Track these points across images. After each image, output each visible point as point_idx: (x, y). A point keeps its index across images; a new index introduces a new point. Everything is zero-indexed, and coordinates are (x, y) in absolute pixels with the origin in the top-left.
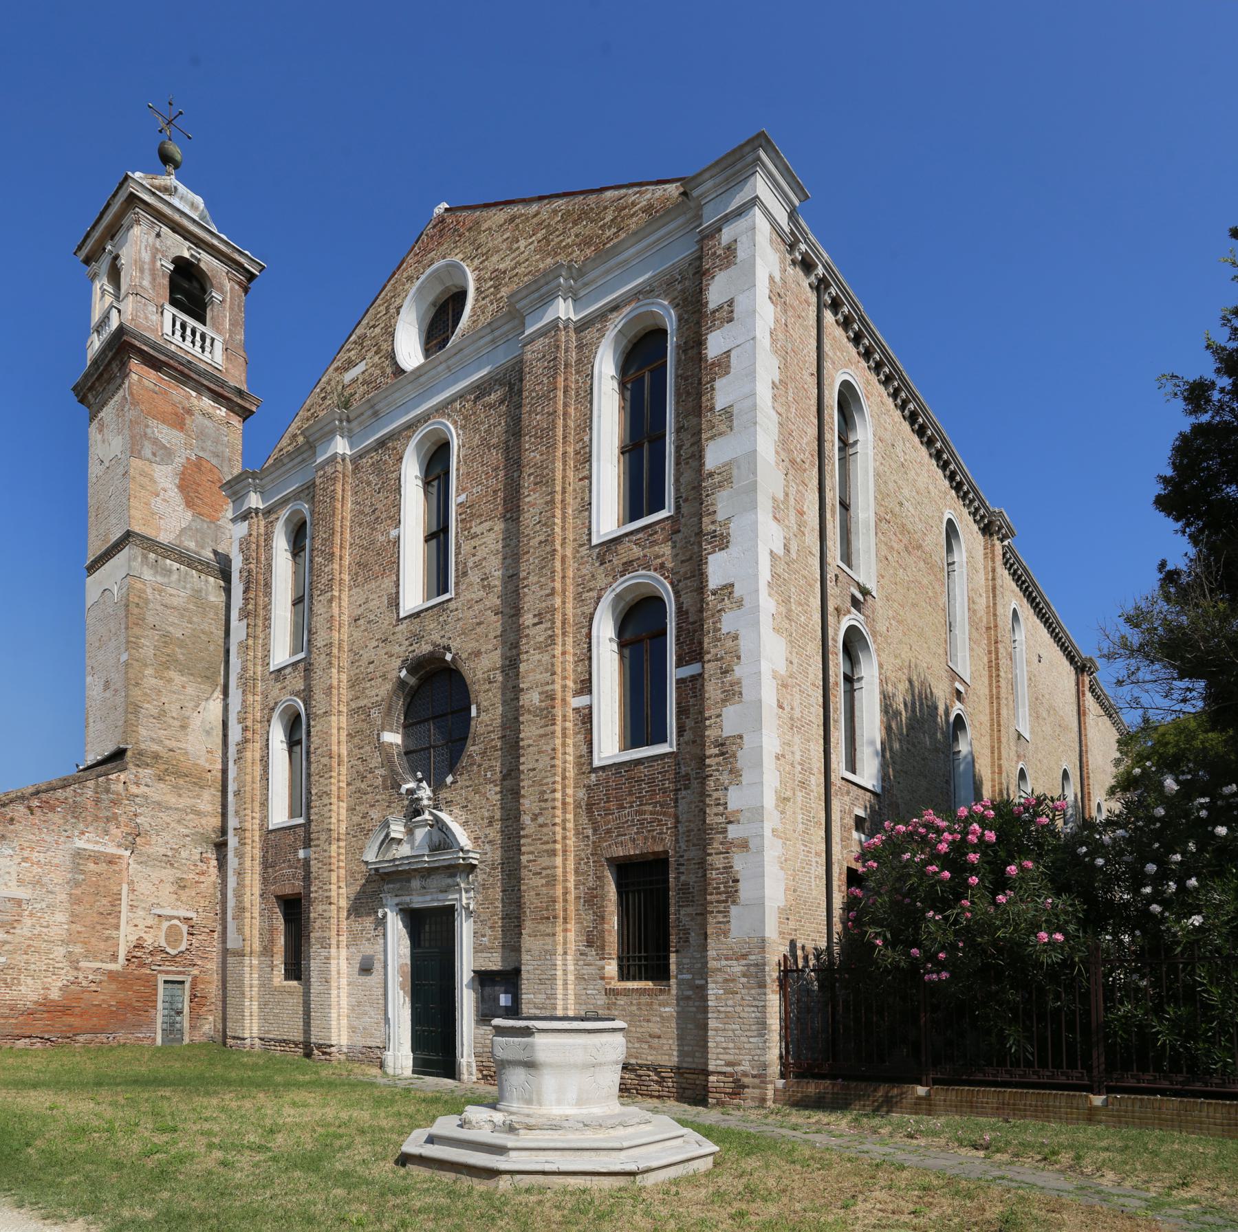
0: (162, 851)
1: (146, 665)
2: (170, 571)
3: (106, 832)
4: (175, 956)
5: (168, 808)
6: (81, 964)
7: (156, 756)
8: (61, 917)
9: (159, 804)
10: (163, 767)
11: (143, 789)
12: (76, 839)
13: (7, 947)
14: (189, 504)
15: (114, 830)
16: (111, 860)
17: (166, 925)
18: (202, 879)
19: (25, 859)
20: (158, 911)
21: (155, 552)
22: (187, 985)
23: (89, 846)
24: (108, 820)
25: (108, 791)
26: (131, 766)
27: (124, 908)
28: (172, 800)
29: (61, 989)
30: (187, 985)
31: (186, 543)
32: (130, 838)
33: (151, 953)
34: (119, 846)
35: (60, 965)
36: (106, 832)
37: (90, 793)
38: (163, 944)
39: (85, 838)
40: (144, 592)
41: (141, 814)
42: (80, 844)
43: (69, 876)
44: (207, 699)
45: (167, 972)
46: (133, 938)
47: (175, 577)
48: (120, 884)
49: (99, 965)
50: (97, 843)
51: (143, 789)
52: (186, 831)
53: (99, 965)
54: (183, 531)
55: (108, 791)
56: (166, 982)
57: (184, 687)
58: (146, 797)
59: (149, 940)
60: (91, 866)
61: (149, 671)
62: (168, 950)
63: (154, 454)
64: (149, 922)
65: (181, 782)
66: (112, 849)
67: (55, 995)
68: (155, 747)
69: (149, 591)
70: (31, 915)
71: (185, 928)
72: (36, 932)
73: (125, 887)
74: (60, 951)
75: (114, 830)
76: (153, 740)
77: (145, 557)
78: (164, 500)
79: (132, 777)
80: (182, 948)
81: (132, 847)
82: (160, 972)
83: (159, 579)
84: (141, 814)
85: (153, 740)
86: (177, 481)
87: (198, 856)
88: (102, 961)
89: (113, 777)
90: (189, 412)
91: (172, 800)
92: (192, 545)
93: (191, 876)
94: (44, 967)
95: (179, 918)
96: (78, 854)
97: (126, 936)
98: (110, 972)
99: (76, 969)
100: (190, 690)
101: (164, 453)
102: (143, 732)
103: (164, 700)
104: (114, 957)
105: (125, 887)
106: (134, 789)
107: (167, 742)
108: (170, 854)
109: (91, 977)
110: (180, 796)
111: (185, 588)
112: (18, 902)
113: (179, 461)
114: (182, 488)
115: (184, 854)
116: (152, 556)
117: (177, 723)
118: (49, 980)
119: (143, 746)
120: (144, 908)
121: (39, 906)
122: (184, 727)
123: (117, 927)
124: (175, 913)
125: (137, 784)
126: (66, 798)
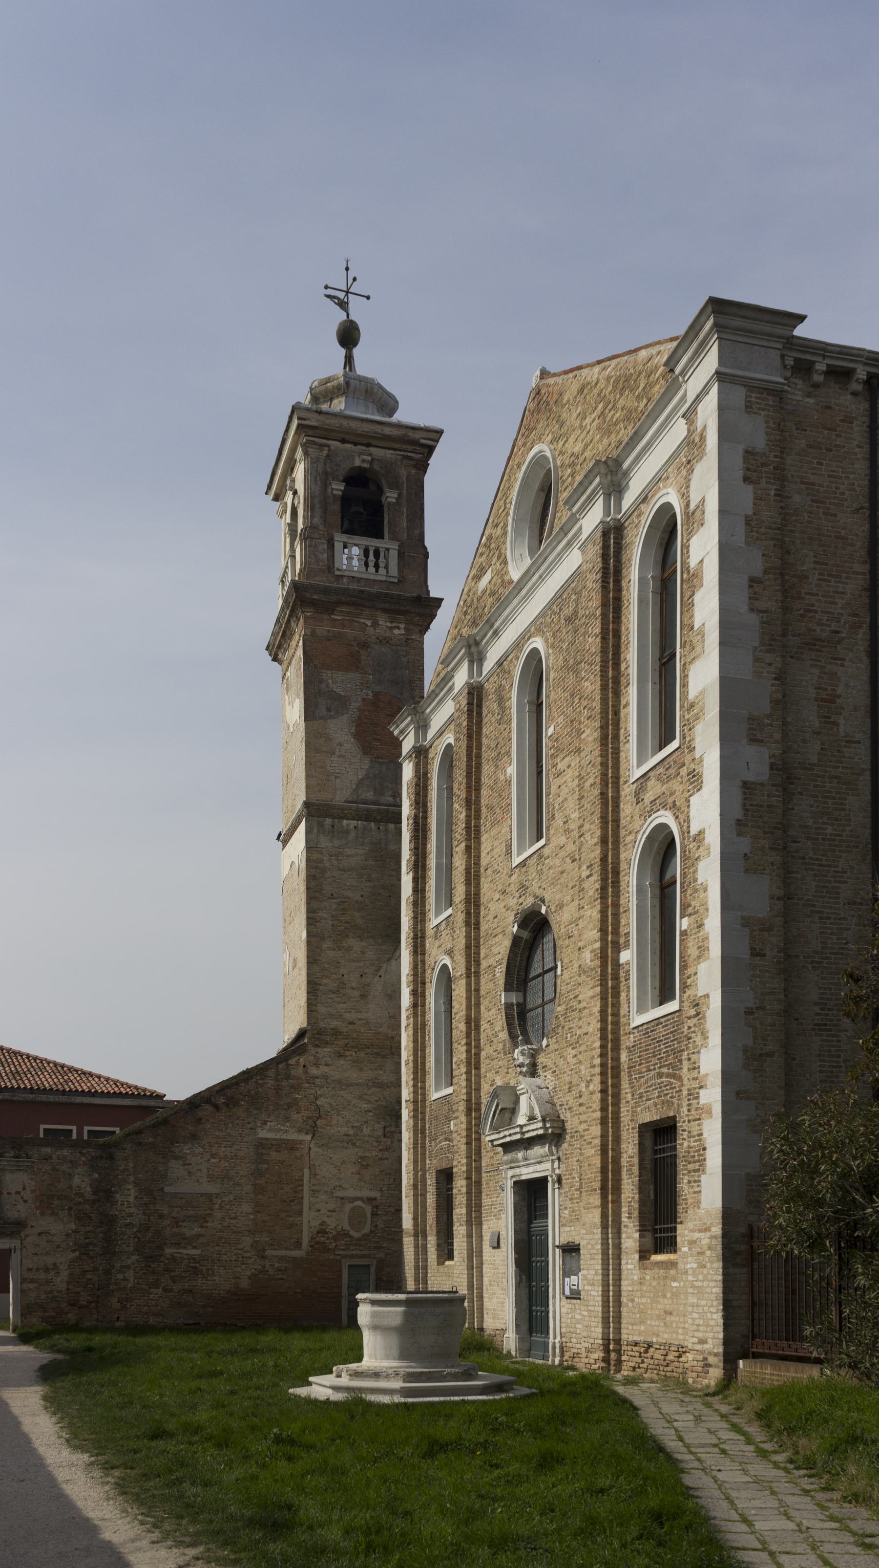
0: (344, 1130)
1: (323, 939)
2: (347, 832)
3: (287, 1119)
4: (360, 1239)
5: (349, 1085)
6: (269, 1252)
7: (336, 1033)
8: (247, 1208)
9: (339, 1082)
10: (342, 1043)
11: (323, 1069)
12: (259, 1130)
13: (201, 1240)
14: (366, 750)
15: (294, 1116)
16: (292, 1146)
17: (348, 1207)
18: (386, 1155)
19: (213, 1156)
20: (340, 1194)
21: (332, 816)
22: (373, 1270)
23: (271, 1135)
24: (289, 1106)
25: (288, 1077)
26: (310, 1047)
27: (306, 1194)
28: (353, 1075)
29: (250, 1278)
30: (373, 1270)
31: (363, 796)
32: (310, 1122)
33: (335, 1238)
34: (300, 1131)
35: (248, 1255)
36: (287, 1119)
37: (270, 1082)
38: (347, 1227)
39: (267, 1127)
40: (321, 861)
41: (321, 1096)
42: (263, 1134)
43: (253, 1167)
44: (389, 960)
45: (352, 1257)
46: (316, 1223)
47: (352, 835)
48: (302, 1170)
49: (283, 1253)
50: (279, 1130)
51: (323, 1069)
52: (366, 1106)
53: (283, 1253)
54: (360, 783)
55: (288, 1077)
56: (349, 1266)
57: (363, 953)
58: (325, 1077)
59: (332, 1223)
60: (274, 1155)
61: (327, 944)
62: (352, 1233)
63: (329, 710)
64: (332, 1206)
65: (362, 1054)
66: (293, 1136)
67: (245, 1283)
68: (335, 1023)
69: (325, 859)
70: (221, 1208)
71: (368, 1209)
72: (225, 1224)
73: (306, 1172)
74: (247, 1241)
75: (294, 1116)
76: (332, 1016)
77: (321, 825)
78: (341, 756)
79: (312, 1058)
80: (367, 1229)
81: (313, 1131)
82: (344, 1257)
83: (336, 842)
84: (321, 1096)
85: (332, 1016)
86: (353, 730)
87: (380, 1133)
88: (286, 1249)
89: (292, 1062)
90: (365, 645)
91: (353, 1075)
92: (370, 795)
93: (374, 1153)
94: (234, 1258)
95: (361, 1199)
96: (262, 1145)
97: (309, 1221)
98: (295, 1259)
99: (264, 1257)
100: (370, 954)
101: (339, 703)
102: (322, 1009)
103: (342, 971)
104: (298, 1244)
105: (306, 1172)
106: (314, 1071)
107: (347, 1016)
108: (351, 1132)
109: (277, 1265)
110: (361, 1070)
111: (363, 844)
112: (210, 1197)
113: (355, 705)
114: (357, 736)
115: (366, 1131)
116: (328, 821)
117: (357, 993)
118: (239, 1269)
119: (322, 1025)
120: (326, 1192)
121: (226, 1199)
122: (363, 996)
123: (300, 1213)
124: (358, 1194)
125: (317, 1065)
126: (249, 1091)
